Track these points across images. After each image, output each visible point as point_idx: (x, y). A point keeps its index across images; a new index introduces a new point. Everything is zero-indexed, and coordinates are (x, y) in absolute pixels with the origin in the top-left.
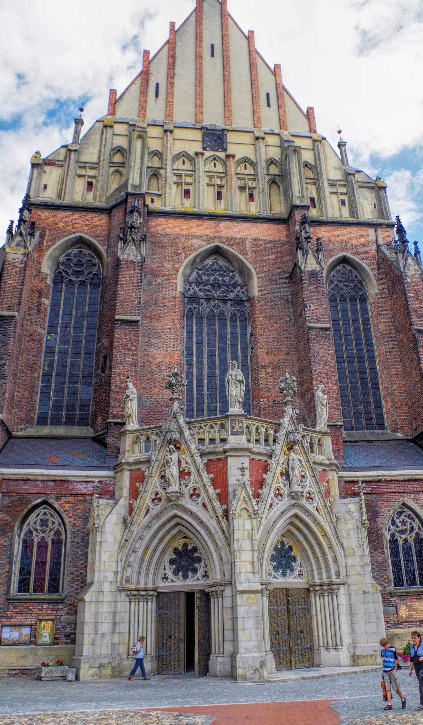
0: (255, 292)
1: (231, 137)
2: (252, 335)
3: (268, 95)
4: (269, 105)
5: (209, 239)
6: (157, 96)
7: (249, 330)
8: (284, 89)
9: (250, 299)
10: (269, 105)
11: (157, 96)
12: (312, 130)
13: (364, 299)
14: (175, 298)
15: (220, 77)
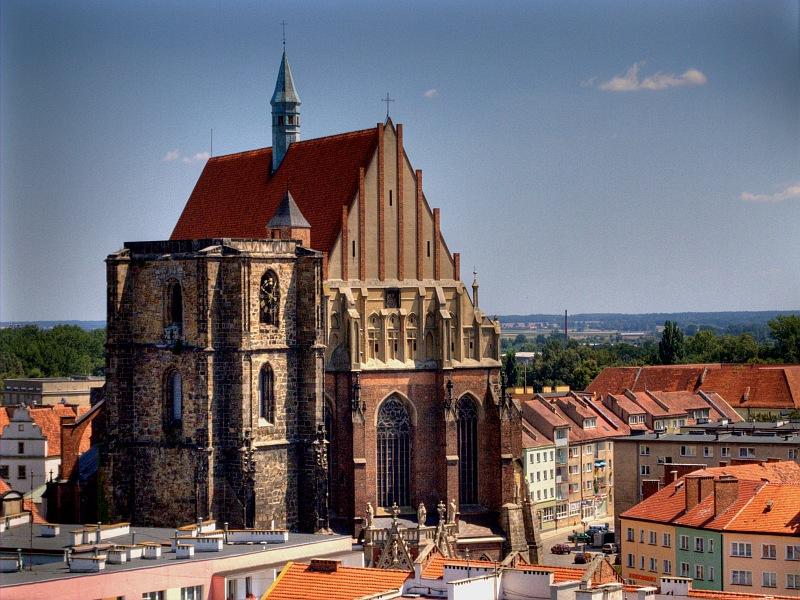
0: (416, 422)
1: (403, 296)
2: (412, 450)
3: (429, 243)
4: (429, 255)
5: (392, 387)
6: (354, 255)
7: (410, 446)
8: (441, 237)
9: (411, 425)
10: (429, 255)
11: (354, 255)
12: (456, 277)
13: (475, 421)
14: (373, 431)
15: (395, 229)
